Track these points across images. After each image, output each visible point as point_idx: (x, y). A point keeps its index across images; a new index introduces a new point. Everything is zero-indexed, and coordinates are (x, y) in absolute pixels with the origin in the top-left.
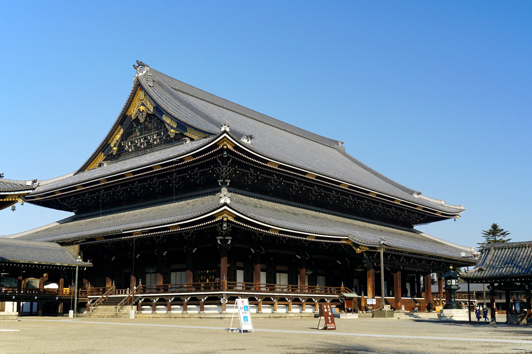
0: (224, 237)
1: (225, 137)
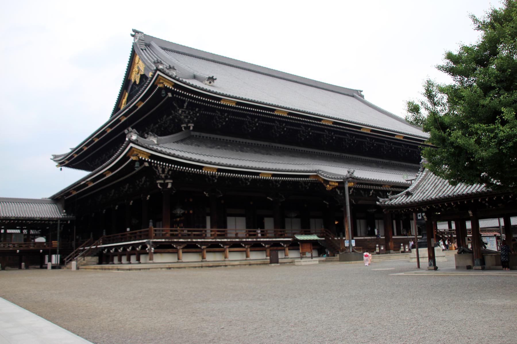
1: (159, 75)
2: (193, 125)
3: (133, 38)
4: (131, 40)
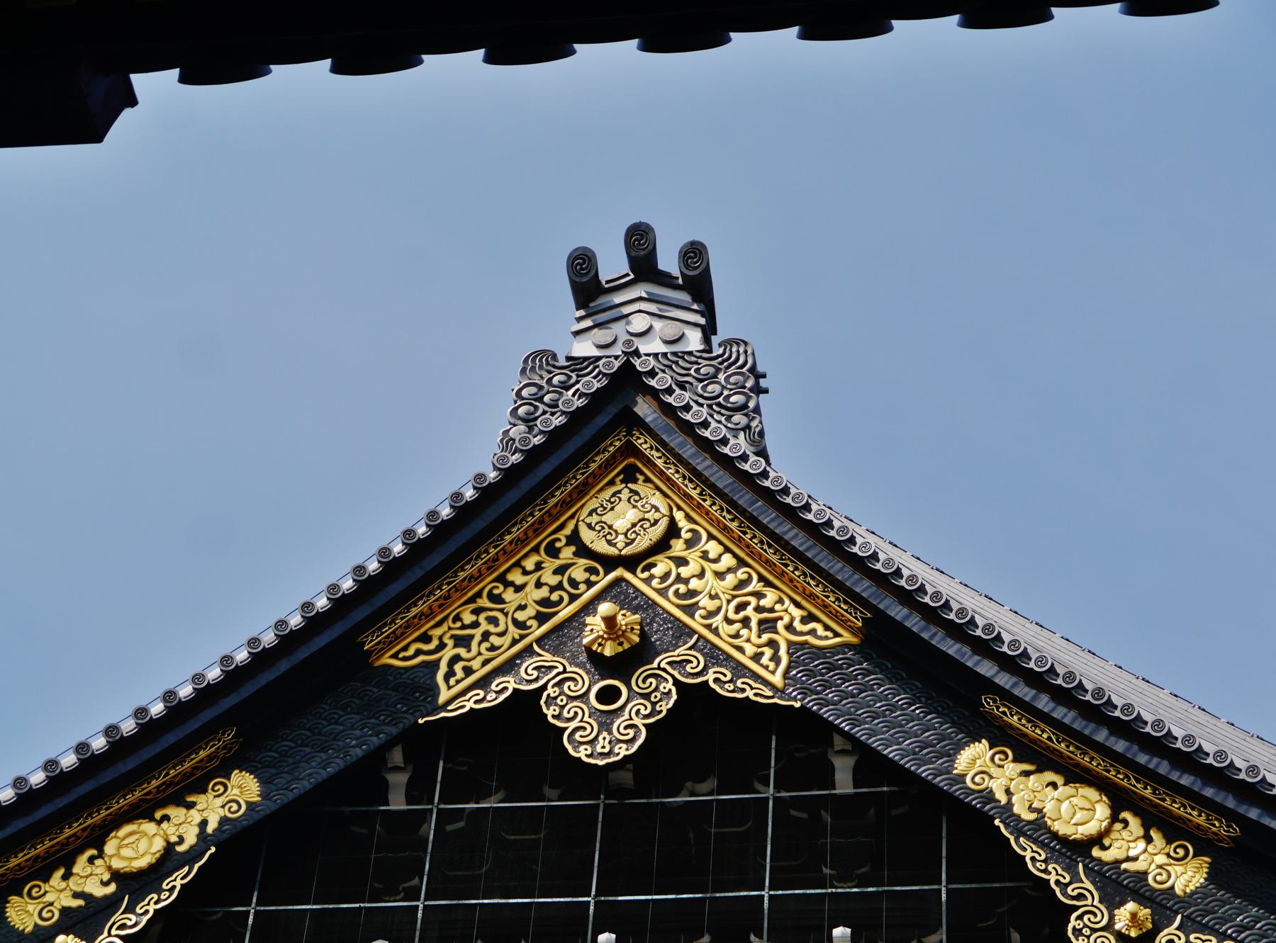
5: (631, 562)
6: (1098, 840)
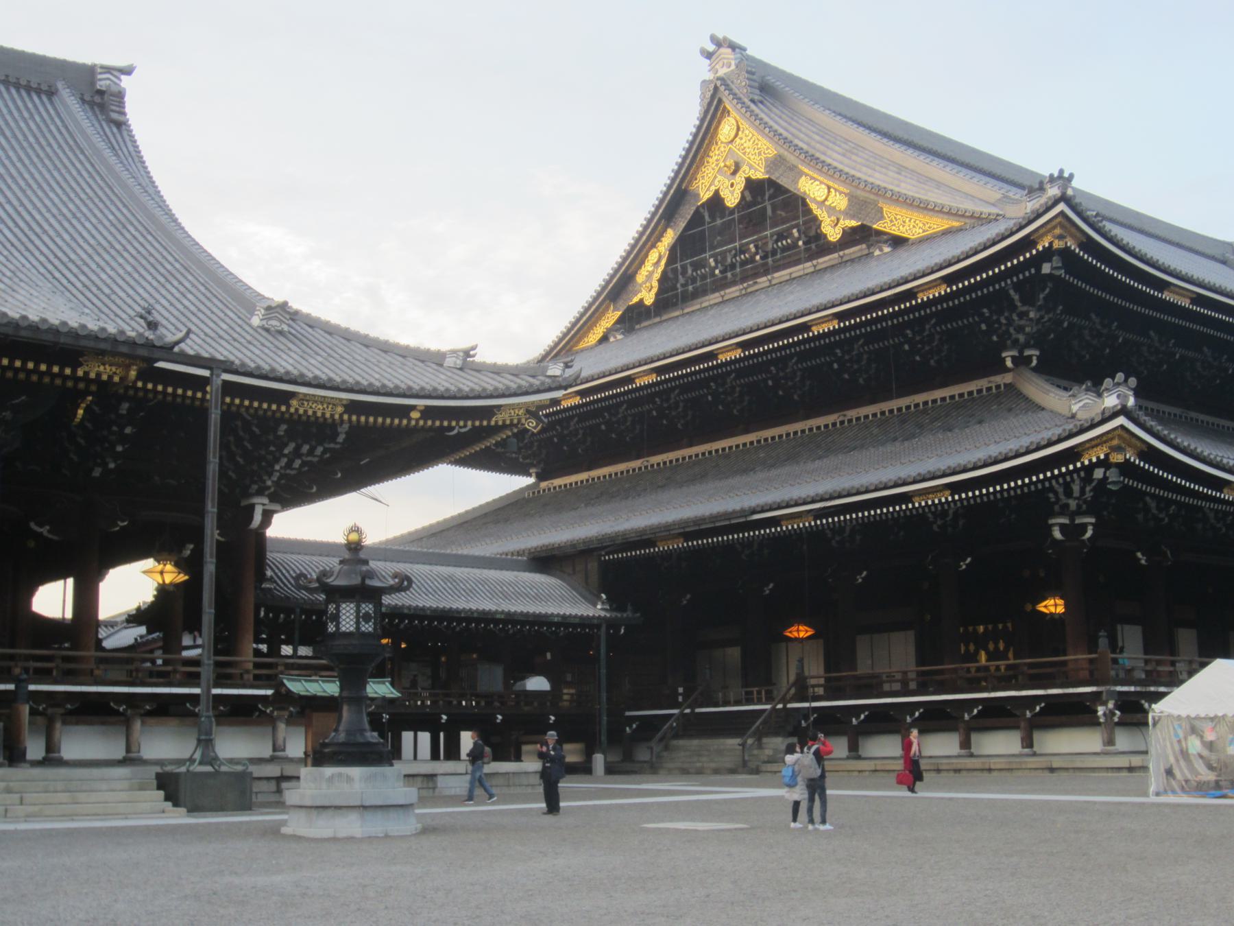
0: (1073, 515)
1: (1062, 213)
2: (1037, 353)
3: (708, 62)
4: (703, 71)
5: (732, 141)
6: (826, 199)
